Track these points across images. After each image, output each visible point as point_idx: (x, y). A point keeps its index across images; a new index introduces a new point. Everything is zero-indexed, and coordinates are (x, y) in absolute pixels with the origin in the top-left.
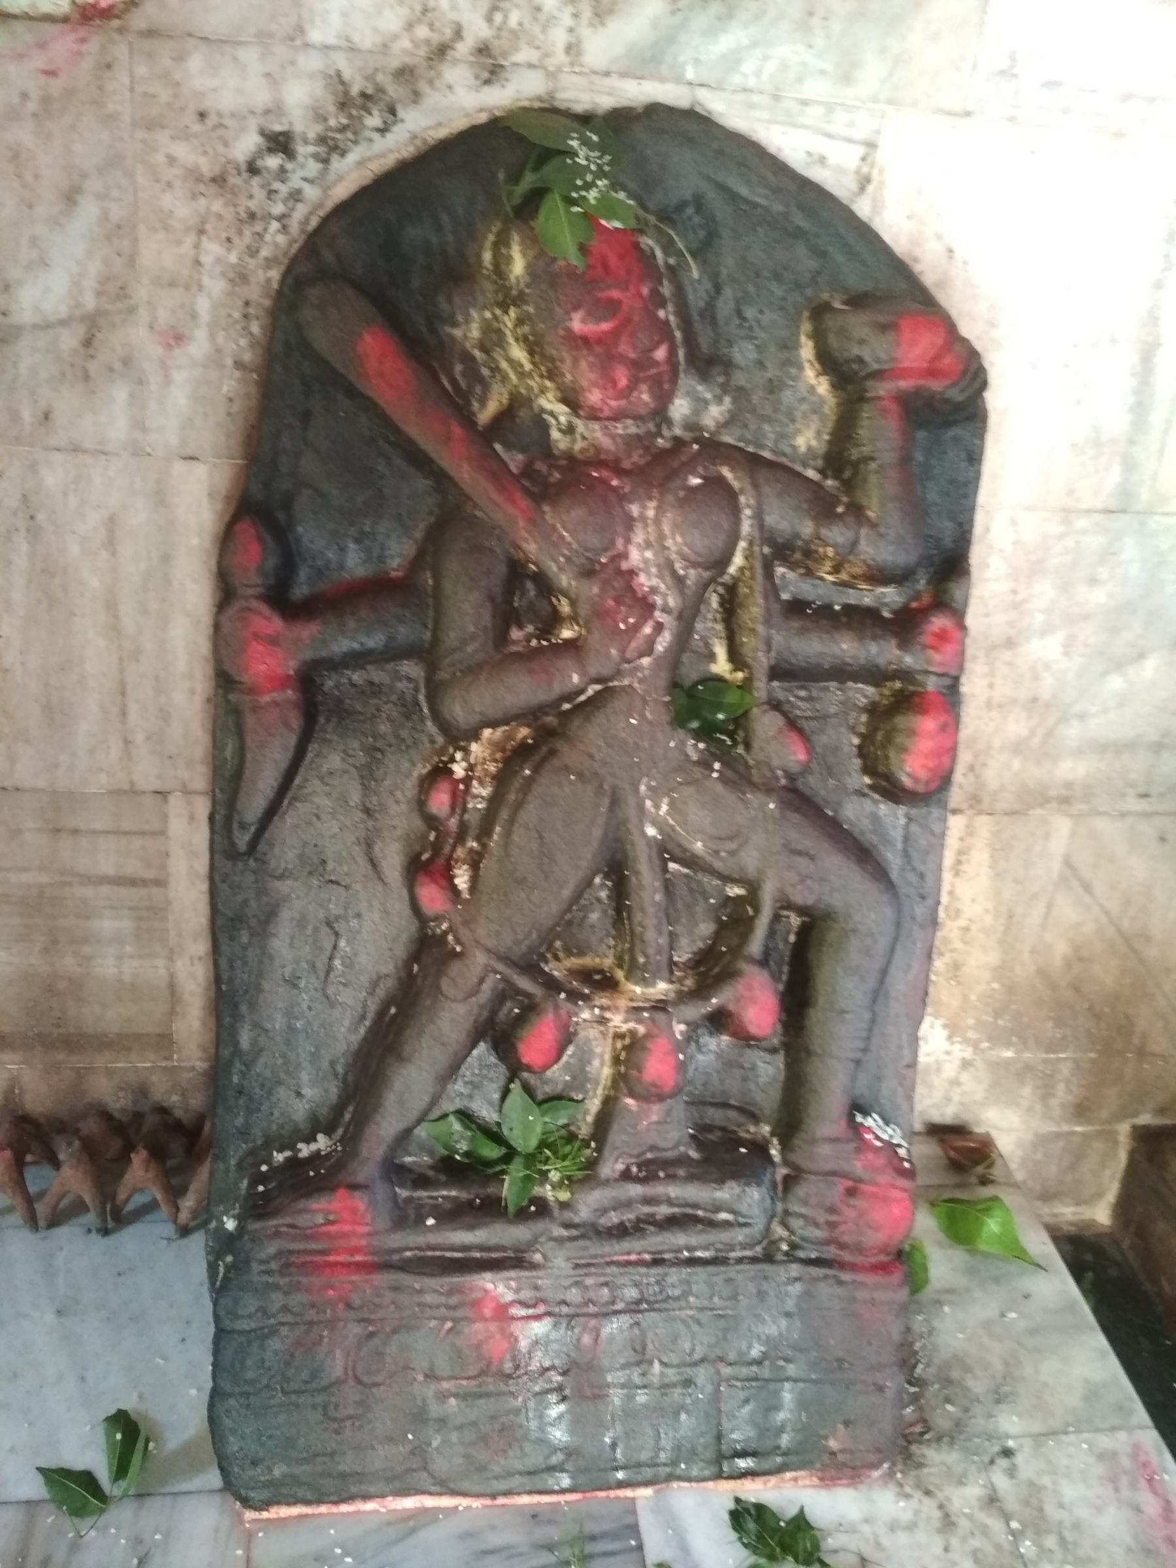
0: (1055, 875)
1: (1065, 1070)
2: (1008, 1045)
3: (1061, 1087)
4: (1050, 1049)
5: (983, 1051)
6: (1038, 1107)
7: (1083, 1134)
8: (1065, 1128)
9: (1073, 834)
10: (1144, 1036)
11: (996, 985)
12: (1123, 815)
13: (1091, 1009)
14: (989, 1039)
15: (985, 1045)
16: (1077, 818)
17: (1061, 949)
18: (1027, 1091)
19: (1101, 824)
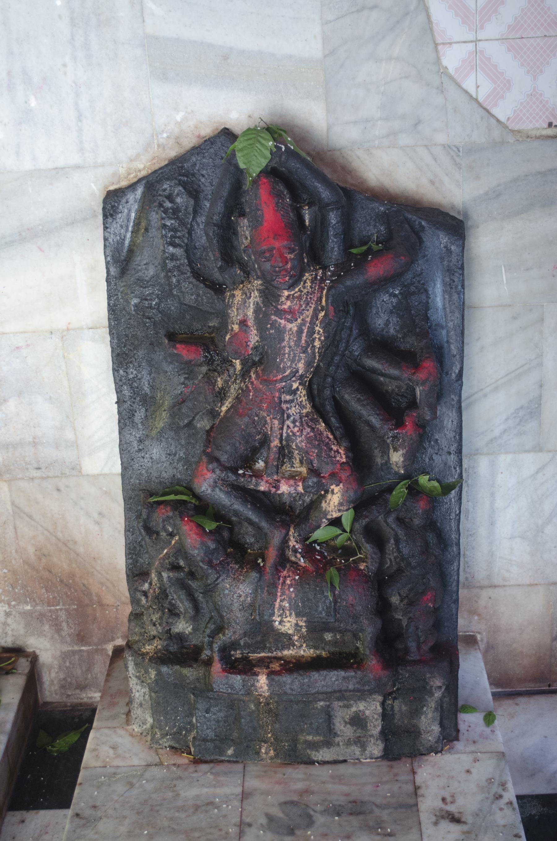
0: (11, 511)
1: (63, 616)
2: (26, 603)
3: (64, 625)
4: (49, 605)
5: (14, 606)
6: (56, 636)
7: (88, 651)
8: (76, 648)
9: (10, 490)
10: (98, 596)
11: (5, 571)
12: (32, 479)
13: (61, 581)
14: (14, 600)
15: (13, 603)
16: (9, 481)
17: (31, 550)
18: (46, 627)
19: (22, 484)
